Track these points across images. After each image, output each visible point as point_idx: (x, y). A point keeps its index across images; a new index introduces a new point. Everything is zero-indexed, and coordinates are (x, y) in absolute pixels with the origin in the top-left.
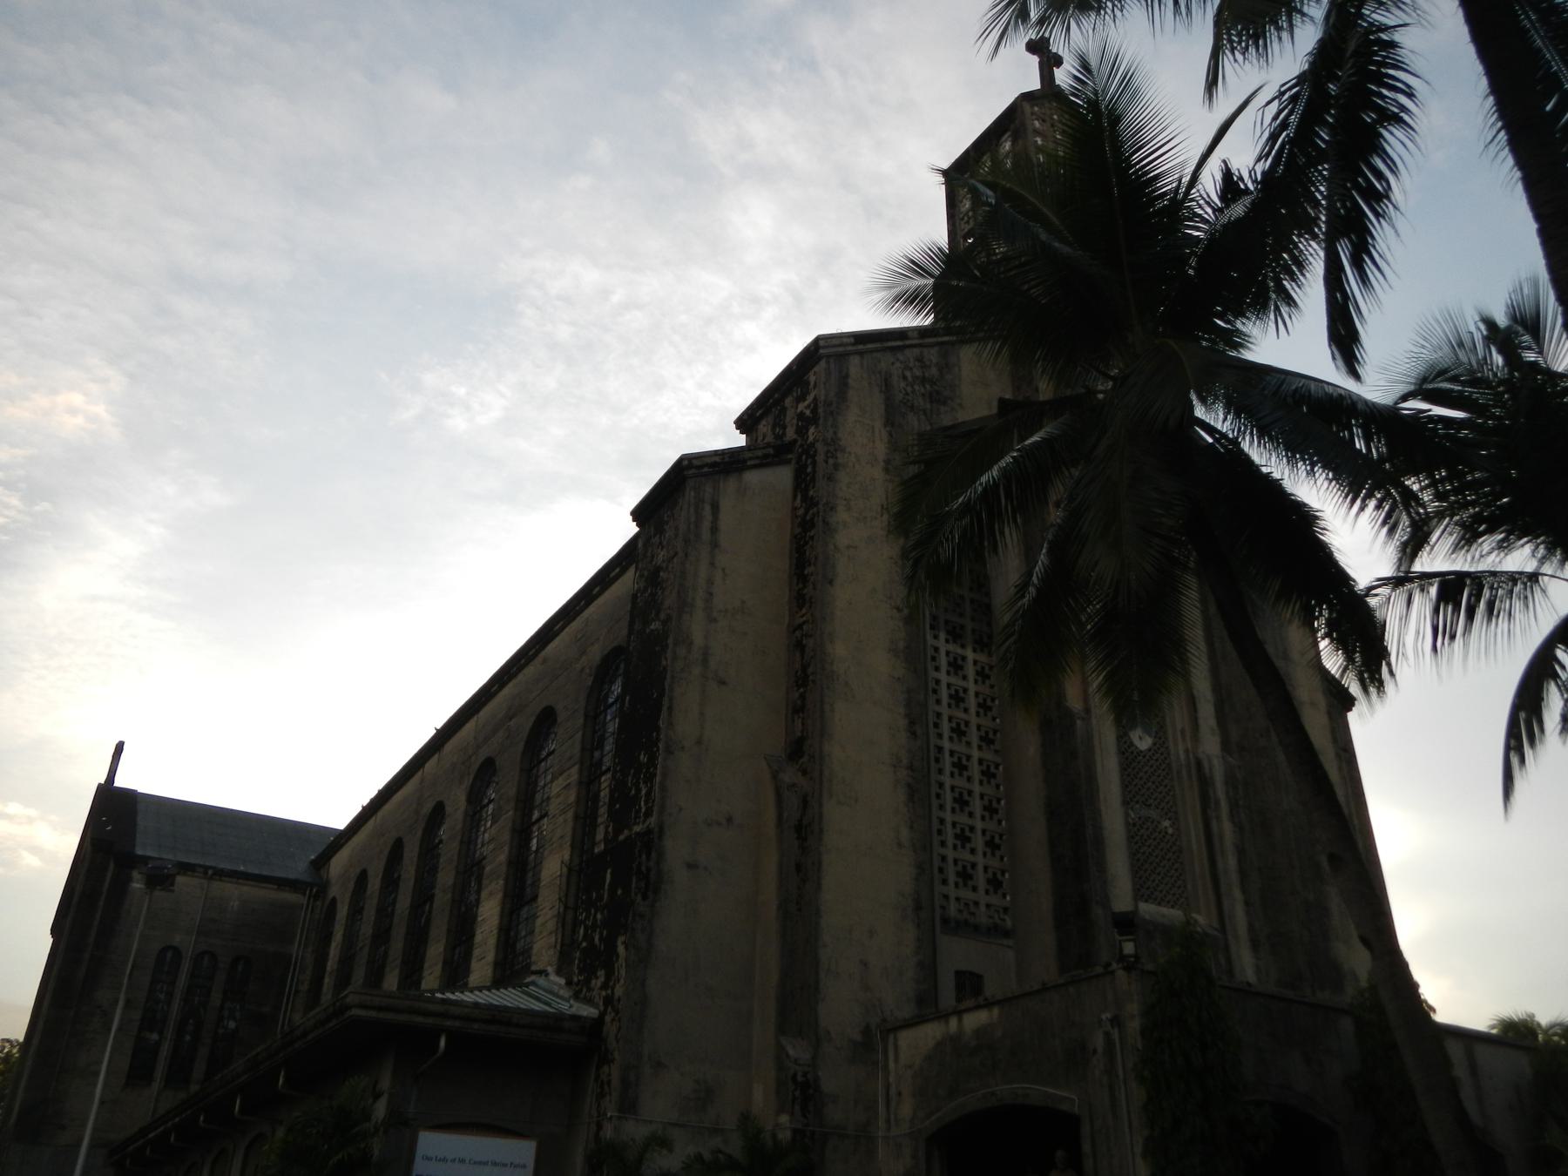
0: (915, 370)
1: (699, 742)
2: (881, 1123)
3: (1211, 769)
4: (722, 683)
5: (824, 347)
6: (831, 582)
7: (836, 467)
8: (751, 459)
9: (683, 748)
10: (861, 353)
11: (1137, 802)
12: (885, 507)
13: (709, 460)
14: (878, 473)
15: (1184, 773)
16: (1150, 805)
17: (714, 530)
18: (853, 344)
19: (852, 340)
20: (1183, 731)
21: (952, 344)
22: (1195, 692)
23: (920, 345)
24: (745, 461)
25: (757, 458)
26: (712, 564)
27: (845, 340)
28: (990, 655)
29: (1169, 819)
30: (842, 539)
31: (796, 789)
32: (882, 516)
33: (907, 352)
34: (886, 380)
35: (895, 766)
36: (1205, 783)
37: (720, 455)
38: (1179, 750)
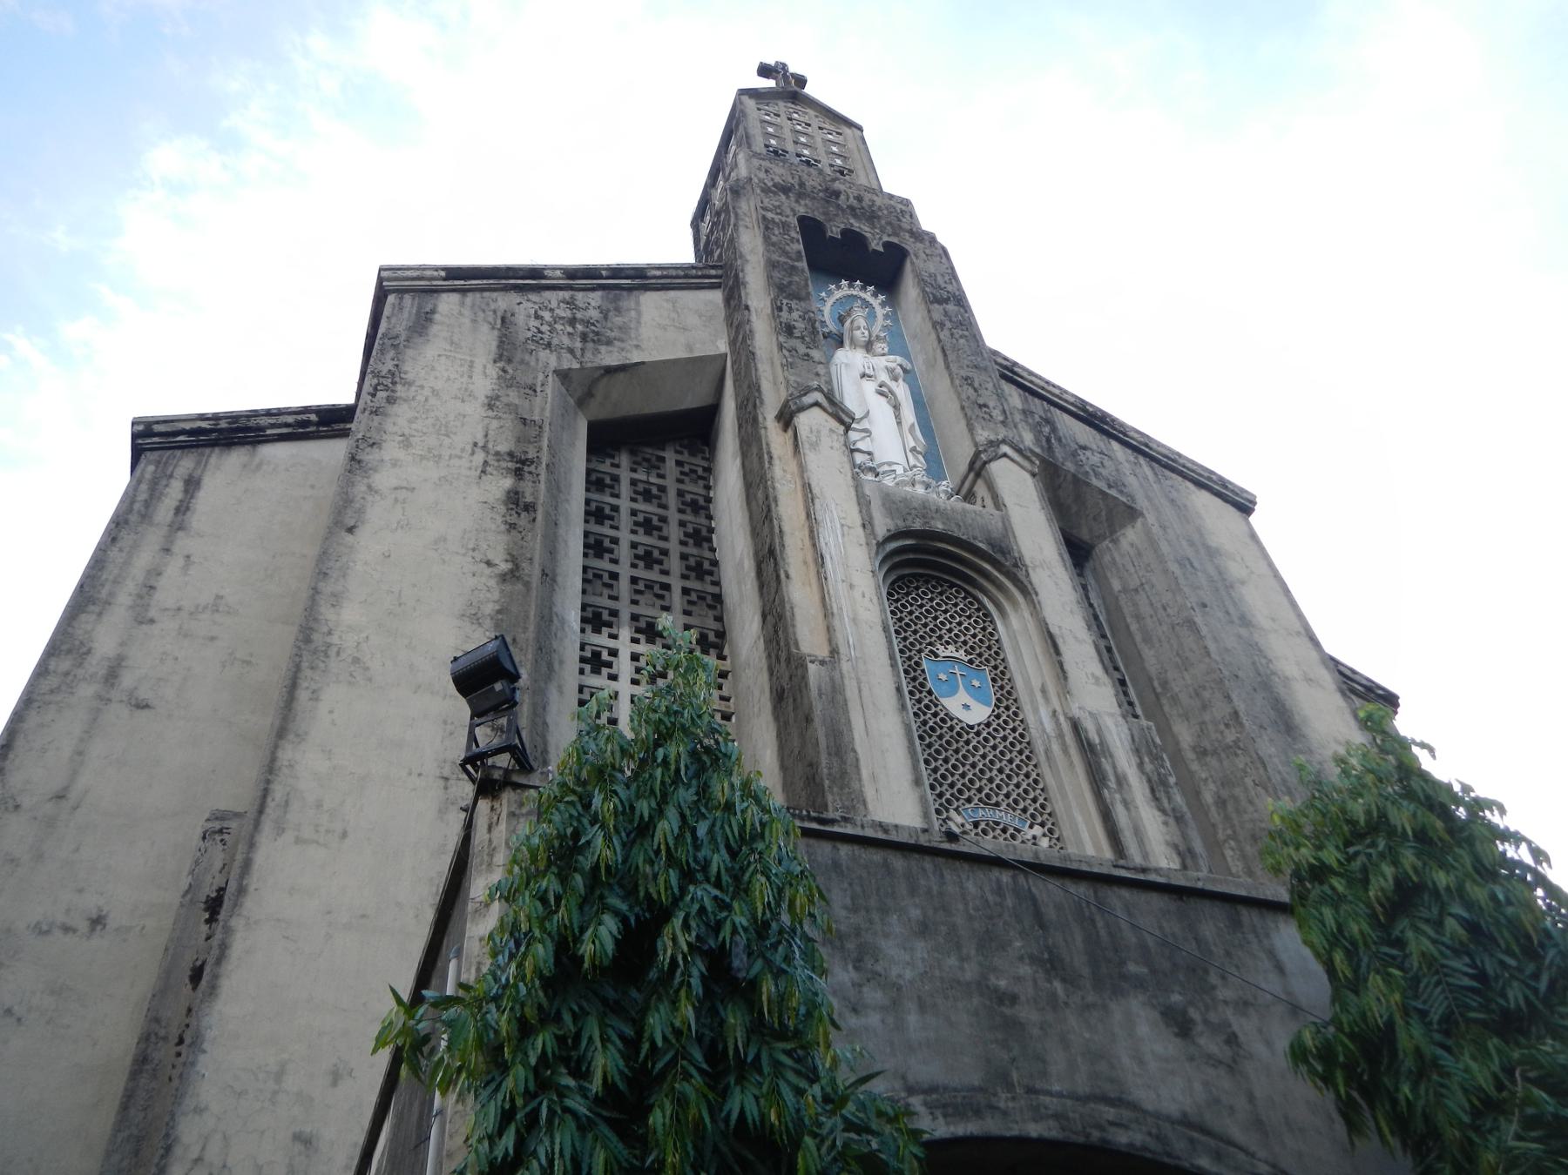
1: (60, 797)
3: (1099, 732)
4: (143, 706)
6: (350, 530)
7: (391, 400)
8: (273, 426)
9: (17, 807)
10: (463, 291)
11: (969, 800)
13: (188, 426)
14: (475, 410)
15: (1056, 747)
16: (997, 804)
17: (182, 509)
18: (445, 279)
19: (443, 274)
20: (1044, 691)
21: (630, 289)
22: (1055, 630)
24: (262, 429)
25: (287, 425)
26: (167, 550)
27: (428, 273)
29: (1042, 825)
31: (226, 837)
32: (473, 453)
33: (547, 294)
34: (503, 319)
36: (1092, 753)
37: (208, 419)
38: (1040, 718)
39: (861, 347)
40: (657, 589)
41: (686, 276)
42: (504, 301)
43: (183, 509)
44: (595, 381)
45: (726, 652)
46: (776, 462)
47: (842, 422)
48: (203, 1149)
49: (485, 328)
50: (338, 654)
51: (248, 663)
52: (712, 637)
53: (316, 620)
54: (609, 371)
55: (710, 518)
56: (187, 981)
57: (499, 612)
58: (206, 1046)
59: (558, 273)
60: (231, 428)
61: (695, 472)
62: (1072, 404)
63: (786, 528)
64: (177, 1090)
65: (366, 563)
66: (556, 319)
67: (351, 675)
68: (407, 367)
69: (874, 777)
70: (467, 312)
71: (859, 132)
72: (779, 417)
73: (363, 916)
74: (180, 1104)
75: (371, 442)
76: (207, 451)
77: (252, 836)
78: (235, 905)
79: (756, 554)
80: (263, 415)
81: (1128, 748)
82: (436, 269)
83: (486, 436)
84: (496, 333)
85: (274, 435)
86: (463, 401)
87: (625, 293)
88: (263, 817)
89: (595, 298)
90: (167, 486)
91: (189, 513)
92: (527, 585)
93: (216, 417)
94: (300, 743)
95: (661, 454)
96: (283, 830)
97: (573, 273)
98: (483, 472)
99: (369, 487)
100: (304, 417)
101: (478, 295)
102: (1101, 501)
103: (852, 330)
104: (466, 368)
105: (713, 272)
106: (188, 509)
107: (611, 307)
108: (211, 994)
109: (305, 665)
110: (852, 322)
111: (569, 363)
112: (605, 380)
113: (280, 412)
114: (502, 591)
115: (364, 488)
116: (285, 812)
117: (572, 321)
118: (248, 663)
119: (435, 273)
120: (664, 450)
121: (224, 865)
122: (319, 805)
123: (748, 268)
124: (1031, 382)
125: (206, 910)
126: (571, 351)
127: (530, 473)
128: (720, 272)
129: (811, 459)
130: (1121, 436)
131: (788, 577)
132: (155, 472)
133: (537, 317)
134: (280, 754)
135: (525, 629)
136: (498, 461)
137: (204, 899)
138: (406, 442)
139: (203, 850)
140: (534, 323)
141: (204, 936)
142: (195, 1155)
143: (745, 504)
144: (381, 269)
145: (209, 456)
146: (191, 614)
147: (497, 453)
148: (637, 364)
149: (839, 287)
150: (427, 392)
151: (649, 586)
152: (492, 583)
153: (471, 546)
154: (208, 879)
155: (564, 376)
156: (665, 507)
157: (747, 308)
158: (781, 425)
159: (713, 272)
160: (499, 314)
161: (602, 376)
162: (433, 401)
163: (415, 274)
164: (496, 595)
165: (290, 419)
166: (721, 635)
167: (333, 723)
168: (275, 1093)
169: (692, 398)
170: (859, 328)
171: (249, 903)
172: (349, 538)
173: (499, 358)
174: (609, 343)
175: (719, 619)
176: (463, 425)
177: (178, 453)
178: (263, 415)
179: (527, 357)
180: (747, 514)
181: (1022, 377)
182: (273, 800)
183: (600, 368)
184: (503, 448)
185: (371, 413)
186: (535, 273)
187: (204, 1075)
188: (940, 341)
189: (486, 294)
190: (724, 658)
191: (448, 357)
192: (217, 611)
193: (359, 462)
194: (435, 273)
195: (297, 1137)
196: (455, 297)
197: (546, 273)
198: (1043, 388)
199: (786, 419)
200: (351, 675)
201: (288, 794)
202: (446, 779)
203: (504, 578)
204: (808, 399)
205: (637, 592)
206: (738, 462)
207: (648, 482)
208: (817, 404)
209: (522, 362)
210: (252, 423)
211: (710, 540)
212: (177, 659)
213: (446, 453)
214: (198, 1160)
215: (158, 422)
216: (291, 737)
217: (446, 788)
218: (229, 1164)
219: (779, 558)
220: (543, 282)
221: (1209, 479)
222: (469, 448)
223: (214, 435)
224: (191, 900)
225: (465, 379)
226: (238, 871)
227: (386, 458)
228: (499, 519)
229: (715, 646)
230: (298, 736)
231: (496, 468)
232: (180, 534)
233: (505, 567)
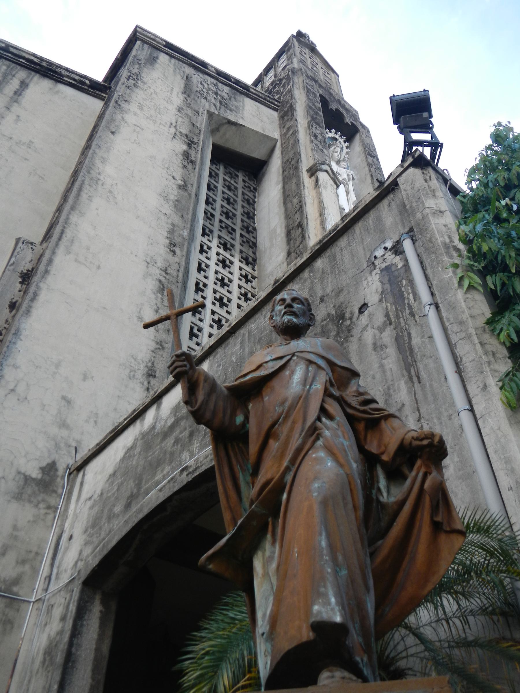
0: (210, 86)
2: (39, 584)
5: (140, 33)
10: (171, 56)
12: (174, 124)
13: (27, 56)
17: (18, 93)
18: (164, 46)
19: (164, 43)
21: (241, 93)
23: (217, 79)
24: (63, 76)
25: (74, 80)
27: (158, 40)
28: (253, 269)
30: (130, 118)
31: (33, 247)
34: (187, 77)
35: (148, 263)
39: (335, 161)
40: (230, 229)
41: (265, 99)
42: (189, 70)
43: (18, 93)
44: (222, 124)
45: (256, 268)
46: (306, 188)
47: (336, 183)
48: (16, 386)
49: (179, 77)
50: (102, 185)
51: (43, 178)
52: (250, 260)
53: (93, 165)
54: (230, 122)
55: (254, 209)
56: (7, 307)
57: (177, 201)
58: (22, 337)
59: (213, 70)
60: (48, 68)
61: (250, 188)
63: (309, 217)
64: (5, 352)
65: (118, 151)
66: (209, 89)
67: (108, 197)
68: (143, 75)
70: (172, 66)
71: (337, 77)
72: (308, 171)
73: (105, 308)
74: (6, 360)
75: (125, 99)
76: (33, 73)
77: (54, 249)
78: (43, 277)
79: (287, 226)
80: (64, 69)
82: (162, 39)
83: (176, 122)
84: (184, 81)
85: (67, 81)
86: (167, 102)
87: (238, 94)
88: (60, 242)
89: (227, 89)
90: (11, 79)
91: (21, 97)
92: (190, 194)
93: (41, 59)
94: (81, 216)
95: (237, 173)
96: (70, 253)
97: (220, 73)
98: (174, 137)
99: (123, 118)
100: (84, 80)
101: (177, 61)
103: (333, 152)
104: (169, 89)
105: (276, 103)
106: (20, 95)
107: (233, 96)
108: (27, 314)
109: (86, 182)
110: (335, 148)
111: (213, 109)
112: (227, 126)
113: (72, 72)
114: (178, 193)
115: (120, 118)
116: (71, 245)
117: (216, 94)
118: (43, 178)
119: (161, 41)
120: (238, 172)
121: (32, 260)
122: (88, 249)
123: (297, 105)
125: (21, 277)
126: (215, 106)
127: (194, 148)
128: (279, 104)
129: (324, 192)
131: (309, 237)
132: (6, 70)
133: (202, 84)
134: (71, 217)
135: (188, 214)
136: (181, 136)
137: (20, 272)
138: (141, 108)
139: (22, 249)
140: (199, 85)
141: (18, 289)
142: (12, 387)
143: (282, 204)
144: (137, 26)
145: (33, 76)
146: (17, 143)
147: (181, 132)
148: (241, 125)
149: (330, 132)
150: (152, 90)
151: (227, 227)
152: (175, 187)
153: (166, 166)
154: (23, 263)
155: (210, 115)
156: (237, 196)
157: (296, 120)
158: (309, 174)
159: (276, 103)
160: (186, 75)
161: (226, 123)
162: (154, 95)
163: (152, 37)
164: (176, 193)
165: (77, 78)
166: (255, 260)
167: (98, 214)
168: (55, 373)
169: (258, 154)
170: (337, 152)
171: (50, 279)
172: (111, 136)
173: (184, 93)
174: (231, 110)
175: (254, 253)
176: (167, 113)
177: (19, 67)
178: (64, 69)
179: (196, 98)
180: (283, 209)
182: (66, 237)
183: (226, 119)
184: (184, 131)
185: (126, 87)
186: (204, 64)
187: (20, 351)
188: (370, 171)
189: (181, 63)
190: (255, 271)
191: (162, 80)
192: (30, 148)
193: (119, 105)
194: (161, 41)
195: (64, 398)
196: (167, 57)
197: (208, 66)
199: (313, 171)
200: (108, 197)
201: (73, 237)
202: (148, 263)
203: (180, 187)
204: (325, 167)
205: (221, 227)
206: (280, 186)
207: (230, 183)
208: (326, 171)
209: (194, 99)
210: (58, 70)
211: (253, 219)
212: (7, 160)
213: (159, 121)
214: (13, 390)
215: (12, 47)
216: (77, 212)
217: (147, 267)
218: (29, 398)
219: (305, 228)
220: (206, 70)
222: (169, 124)
223: (38, 67)
224: (14, 269)
225: (169, 94)
226: (46, 262)
227: (131, 110)
228: (180, 161)
229: (252, 264)
230: (80, 212)
231: (180, 138)
232: (15, 104)
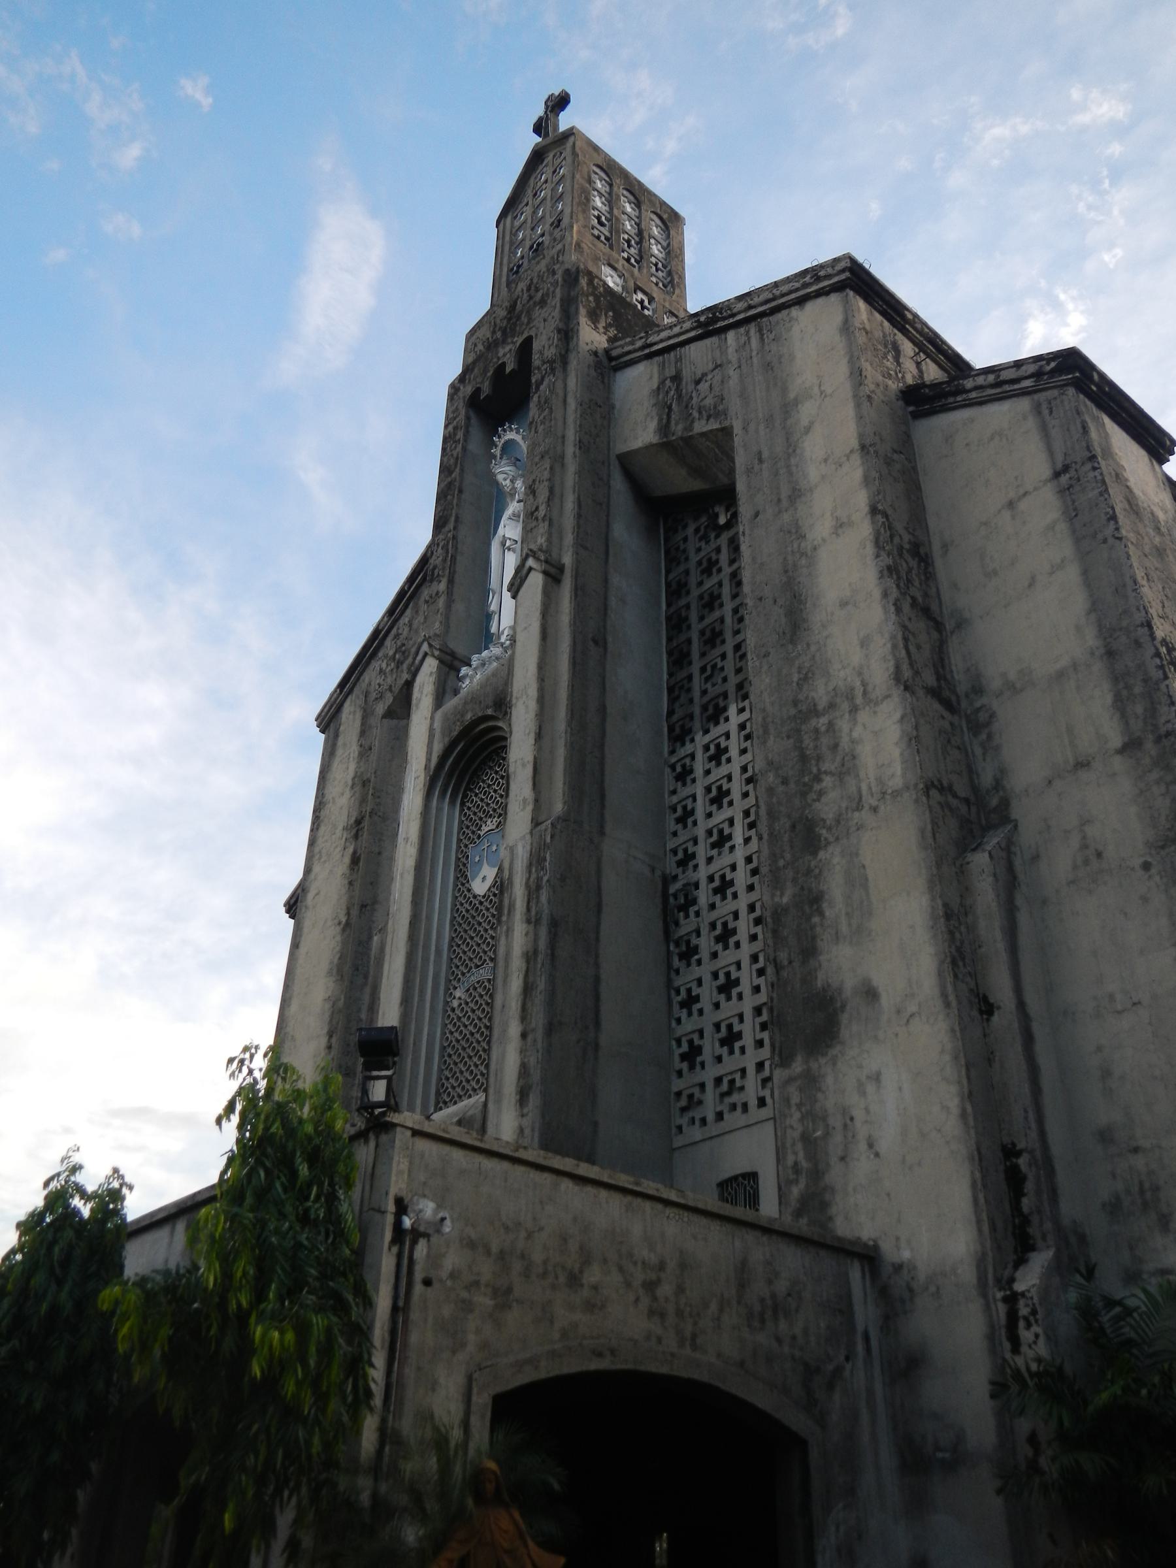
59: (386, 619)
62: (692, 329)
69: (384, 1014)
81: (525, 865)
102: (707, 443)
124: (662, 341)
130: (731, 320)
163: (329, 705)
181: (655, 344)
198: (670, 338)
221: (805, 286)
233: (344, 920)
